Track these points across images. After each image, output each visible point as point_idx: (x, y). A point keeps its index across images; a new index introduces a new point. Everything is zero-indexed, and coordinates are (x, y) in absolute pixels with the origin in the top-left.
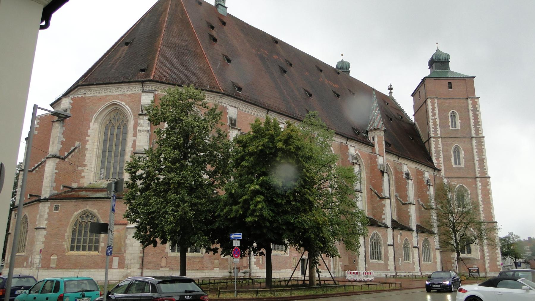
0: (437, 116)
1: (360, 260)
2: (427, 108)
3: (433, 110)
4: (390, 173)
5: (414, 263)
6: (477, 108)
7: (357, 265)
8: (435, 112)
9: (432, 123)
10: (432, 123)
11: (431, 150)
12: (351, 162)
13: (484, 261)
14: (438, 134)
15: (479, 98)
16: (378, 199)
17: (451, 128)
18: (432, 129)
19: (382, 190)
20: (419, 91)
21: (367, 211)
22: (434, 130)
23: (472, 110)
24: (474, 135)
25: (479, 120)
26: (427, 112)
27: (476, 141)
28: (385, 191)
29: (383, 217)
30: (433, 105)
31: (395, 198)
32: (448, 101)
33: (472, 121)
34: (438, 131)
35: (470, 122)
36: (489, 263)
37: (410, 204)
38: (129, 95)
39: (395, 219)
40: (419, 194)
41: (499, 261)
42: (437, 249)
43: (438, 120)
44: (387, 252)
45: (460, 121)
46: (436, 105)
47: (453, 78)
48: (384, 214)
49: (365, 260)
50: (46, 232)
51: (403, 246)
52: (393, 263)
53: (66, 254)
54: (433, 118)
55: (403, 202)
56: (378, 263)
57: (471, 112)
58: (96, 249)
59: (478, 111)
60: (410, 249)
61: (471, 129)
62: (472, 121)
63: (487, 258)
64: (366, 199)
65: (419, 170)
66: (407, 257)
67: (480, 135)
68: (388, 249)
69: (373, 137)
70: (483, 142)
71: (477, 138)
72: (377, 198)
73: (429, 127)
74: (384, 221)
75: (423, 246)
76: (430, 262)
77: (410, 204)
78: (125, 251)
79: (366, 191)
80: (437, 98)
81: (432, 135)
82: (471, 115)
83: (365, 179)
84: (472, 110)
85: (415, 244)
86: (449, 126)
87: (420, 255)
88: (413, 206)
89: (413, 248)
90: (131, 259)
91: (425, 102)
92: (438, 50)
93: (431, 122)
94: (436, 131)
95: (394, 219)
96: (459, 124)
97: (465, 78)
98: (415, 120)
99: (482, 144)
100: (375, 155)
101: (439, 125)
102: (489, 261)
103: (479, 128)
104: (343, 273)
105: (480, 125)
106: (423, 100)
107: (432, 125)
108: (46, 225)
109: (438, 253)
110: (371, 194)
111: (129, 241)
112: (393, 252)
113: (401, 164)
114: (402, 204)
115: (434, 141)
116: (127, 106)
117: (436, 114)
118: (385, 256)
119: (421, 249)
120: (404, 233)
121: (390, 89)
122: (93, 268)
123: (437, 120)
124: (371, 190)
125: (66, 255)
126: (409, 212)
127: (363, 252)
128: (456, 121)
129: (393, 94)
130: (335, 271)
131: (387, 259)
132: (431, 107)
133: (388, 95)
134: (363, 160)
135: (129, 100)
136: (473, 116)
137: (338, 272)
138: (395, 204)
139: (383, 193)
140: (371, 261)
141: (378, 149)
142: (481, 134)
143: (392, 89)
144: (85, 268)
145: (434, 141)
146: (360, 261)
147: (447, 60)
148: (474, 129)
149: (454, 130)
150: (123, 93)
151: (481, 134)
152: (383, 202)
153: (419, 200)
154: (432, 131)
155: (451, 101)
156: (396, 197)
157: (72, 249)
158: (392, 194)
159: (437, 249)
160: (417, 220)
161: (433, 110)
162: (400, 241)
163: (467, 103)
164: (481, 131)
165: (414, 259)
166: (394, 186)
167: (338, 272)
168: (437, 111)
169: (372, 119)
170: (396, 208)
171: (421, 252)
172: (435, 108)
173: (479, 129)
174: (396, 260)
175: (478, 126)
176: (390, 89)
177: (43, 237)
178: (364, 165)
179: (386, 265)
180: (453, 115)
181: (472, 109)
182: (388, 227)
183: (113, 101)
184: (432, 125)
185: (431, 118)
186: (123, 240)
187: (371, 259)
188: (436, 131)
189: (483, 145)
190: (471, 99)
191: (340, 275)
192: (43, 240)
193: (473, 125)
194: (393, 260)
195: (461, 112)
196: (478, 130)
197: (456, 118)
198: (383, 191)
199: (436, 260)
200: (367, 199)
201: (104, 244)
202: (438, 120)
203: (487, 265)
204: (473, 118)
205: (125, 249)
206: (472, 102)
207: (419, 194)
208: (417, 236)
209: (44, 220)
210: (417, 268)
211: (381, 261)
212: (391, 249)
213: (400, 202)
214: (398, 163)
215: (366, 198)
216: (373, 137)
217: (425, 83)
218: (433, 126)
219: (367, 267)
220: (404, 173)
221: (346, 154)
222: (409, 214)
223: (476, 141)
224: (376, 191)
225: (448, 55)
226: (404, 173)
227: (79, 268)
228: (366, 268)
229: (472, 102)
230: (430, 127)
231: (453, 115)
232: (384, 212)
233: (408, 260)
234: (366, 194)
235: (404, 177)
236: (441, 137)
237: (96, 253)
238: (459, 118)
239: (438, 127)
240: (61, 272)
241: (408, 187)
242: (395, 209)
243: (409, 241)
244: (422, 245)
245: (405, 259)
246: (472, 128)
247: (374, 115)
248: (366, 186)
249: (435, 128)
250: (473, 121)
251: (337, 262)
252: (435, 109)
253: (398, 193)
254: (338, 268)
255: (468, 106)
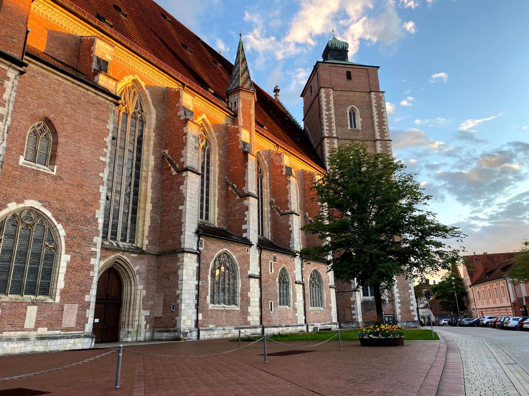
0: (333, 111)
1: (183, 305)
2: (319, 102)
3: (328, 103)
4: (263, 167)
5: (295, 310)
6: (381, 104)
7: (178, 316)
8: (330, 106)
9: (326, 119)
10: (326, 119)
11: (324, 155)
12: (182, 118)
13: (393, 305)
14: (333, 134)
15: (384, 92)
16: (238, 198)
17: (349, 128)
18: (325, 128)
19: (244, 183)
20: (310, 86)
21: (218, 219)
22: (328, 128)
23: (376, 107)
24: (378, 137)
25: (384, 119)
26: (320, 106)
27: (381, 145)
28: (249, 185)
29: (244, 227)
30: (328, 96)
31: (269, 206)
32: (346, 93)
33: (376, 120)
34: (333, 130)
35: (373, 121)
36: (400, 308)
37: (292, 213)
39: (268, 235)
40: (307, 206)
41: (412, 305)
42: (330, 287)
43: (333, 116)
44: (246, 289)
45: (361, 120)
46: (331, 98)
47: (352, 66)
48: (245, 223)
49: (197, 305)
51: (277, 280)
52: (258, 309)
54: (327, 113)
55: (282, 211)
56: (227, 311)
57: (374, 109)
59: (383, 108)
60: (291, 286)
61: (374, 131)
62: (376, 120)
63: (397, 300)
64: (217, 198)
65: (307, 172)
66: (285, 300)
67: (386, 138)
68: (249, 285)
69: (235, 103)
70: (389, 147)
71: (382, 142)
72: (235, 197)
73: (321, 125)
74: (244, 235)
75: (310, 281)
76: (322, 308)
77: (292, 213)
79: (217, 183)
80: (333, 88)
81: (326, 135)
82: (375, 112)
83: (217, 165)
84: (376, 107)
85: (299, 278)
86: (348, 125)
87: (306, 295)
88: (297, 217)
89: (294, 284)
91: (318, 95)
92: (334, 38)
93: (324, 119)
94: (330, 130)
95: (267, 238)
96: (360, 124)
97: (368, 68)
98: (305, 125)
99: (389, 149)
100: (236, 127)
101: (334, 123)
102: (399, 305)
103: (385, 129)
104: (148, 335)
105: (385, 125)
106: (314, 94)
107: (326, 122)
109: (333, 292)
110: (228, 190)
112: (259, 289)
113: (280, 155)
114: (279, 215)
115: (328, 143)
117: (331, 108)
118: (242, 298)
119: (307, 286)
120: (280, 257)
121: (276, 91)
123: (332, 116)
124: (228, 185)
126: (290, 226)
127: (194, 287)
128: (356, 120)
129: (278, 98)
130: (130, 329)
131: (247, 302)
132: (326, 100)
133: (274, 98)
134: (215, 133)
136: (377, 114)
137: (137, 331)
138: (269, 216)
139: (246, 187)
140: (211, 306)
141: (242, 120)
142: (387, 136)
143: (278, 91)
145: (328, 143)
146: (183, 306)
147: (346, 49)
148: (379, 130)
149: (354, 131)
151: (387, 136)
152: (245, 202)
153: (307, 214)
154: (326, 130)
155: (350, 94)
156: (271, 203)
158: (266, 200)
159: (330, 287)
160: (303, 244)
161: (328, 103)
162: (273, 271)
163: (370, 98)
164: (387, 133)
165: (296, 303)
166: (269, 187)
167: (137, 331)
168: (332, 105)
169: (235, 77)
170: (270, 220)
171: (308, 291)
172: (331, 101)
173: (385, 130)
174: (264, 305)
175: (383, 127)
176: (276, 91)
178: (217, 141)
179: (245, 313)
180: (352, 112)
181: (376, 105)
182: (251, 245)
184: (326, 122)
185: (324, 112)
187: (213, 302)
188: (330, 130)
189: (390, 151)
190: (374, 93)
191: (141, 338)
193: (377, 126)
194: (258, 304)
195: (362, 109)
196: (383, 132)
197: (356, 116)
198: (246, 184)
199: (330, 305)
200: (218, 198)
202: (333, 116)
203: (398, 311)
204: (378, 116)
206: (375, 96)
207: (307, 206)
208: (302, 265)
210: (301, 319)
211: (233, 306)
212: (254, 284)
213: (277, 212)
214: (277, 153)
215: (217, 195)
216: (235, 103)
217: (318, 71)
218: (328, 124)
219: (200, 317)
220: (284, 167)
221: (175, 106)
222: (290, 229)
223: (381, 145)
224: (234, 185)
225: (347, 44)
226: (284, 167)
228: (197, 321)
229: (375, 96)
230: (323, 125)
231: (353, 114)
232: (246, 219)
233: (287, 305)
234: (217, 189)
235: (284, 173)
236: (337, 138)
238: (360, 116)
239: (334, 124)
241: (290, 188)
242: (270, 222)
243: (288, 272)
244: (309, 280)
245: (280, 300)
246: (377, 129)
247: (239, 70)
248: (217, 175)
249: (330, 126)
250: (378, 120)
251: (137, 311)
252: (330, 102)
253: (274, 198)
254: (136, 323)
255: (371, 102)
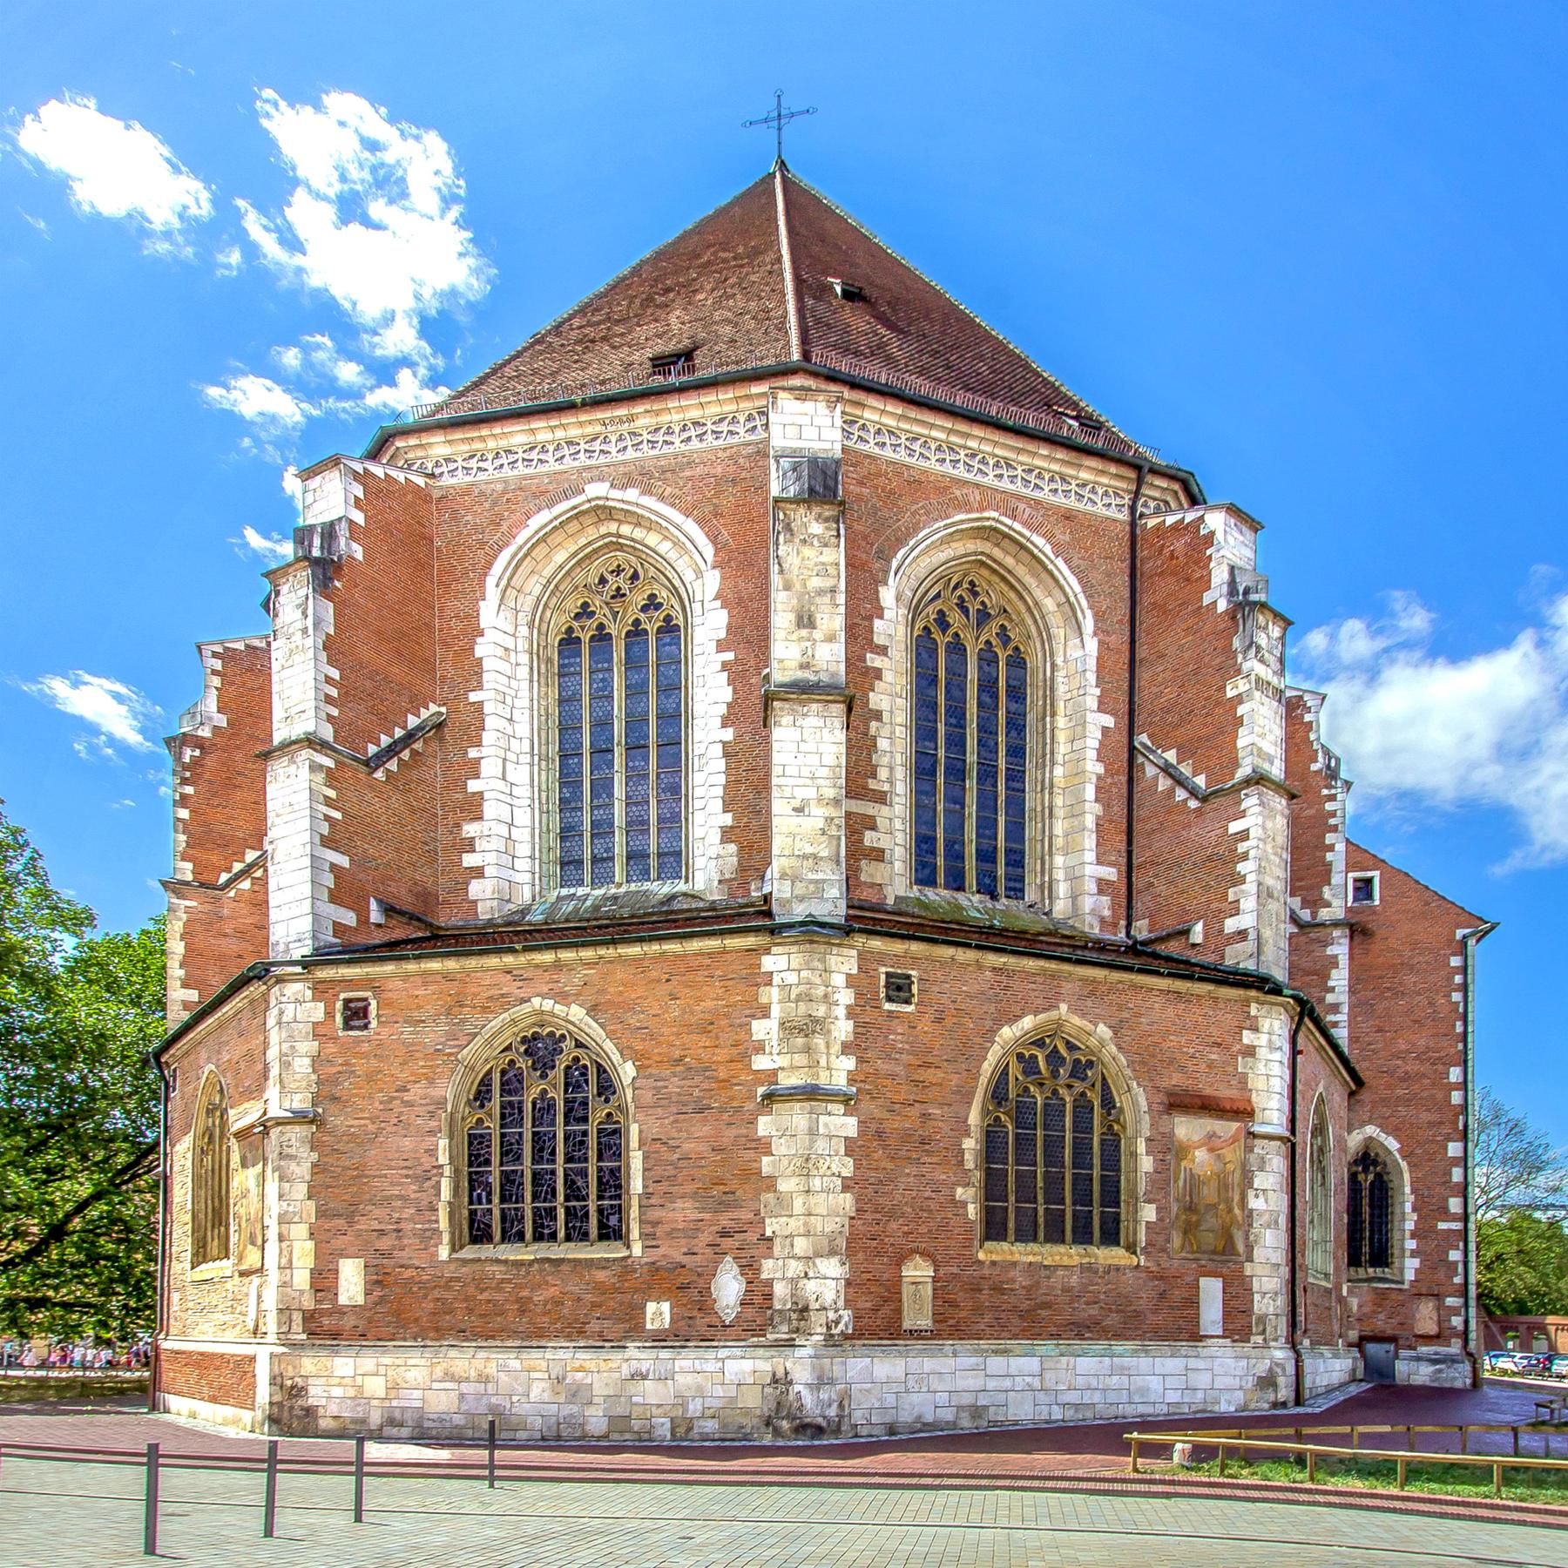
38: (1068, 516)
50: (852, 1121)
53: (981, 1256)
58: (1111, 1236)
78: (1250, 1248)
90: (1276, 1294)
108: (851, 1081)
111: (1261, 1199)
116: (1060, 562)
122: (1118, 1336)
125: (981, 1263)
135: (1067, 538)
144: (1080, 1336)
150: (1037, 494)
157: (994, 1228)
177: (842, 1151)
183: (986, 514)
186: (1237, 1198)
192: (847, 1168)
201: (1159, 1210)
205: (1247, 1238)
209: (836, 1048)
227: (1052, 1336)
237: (1114, 1255)
240: (973, 1360)
